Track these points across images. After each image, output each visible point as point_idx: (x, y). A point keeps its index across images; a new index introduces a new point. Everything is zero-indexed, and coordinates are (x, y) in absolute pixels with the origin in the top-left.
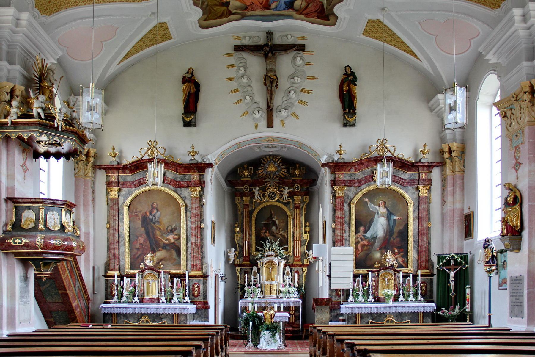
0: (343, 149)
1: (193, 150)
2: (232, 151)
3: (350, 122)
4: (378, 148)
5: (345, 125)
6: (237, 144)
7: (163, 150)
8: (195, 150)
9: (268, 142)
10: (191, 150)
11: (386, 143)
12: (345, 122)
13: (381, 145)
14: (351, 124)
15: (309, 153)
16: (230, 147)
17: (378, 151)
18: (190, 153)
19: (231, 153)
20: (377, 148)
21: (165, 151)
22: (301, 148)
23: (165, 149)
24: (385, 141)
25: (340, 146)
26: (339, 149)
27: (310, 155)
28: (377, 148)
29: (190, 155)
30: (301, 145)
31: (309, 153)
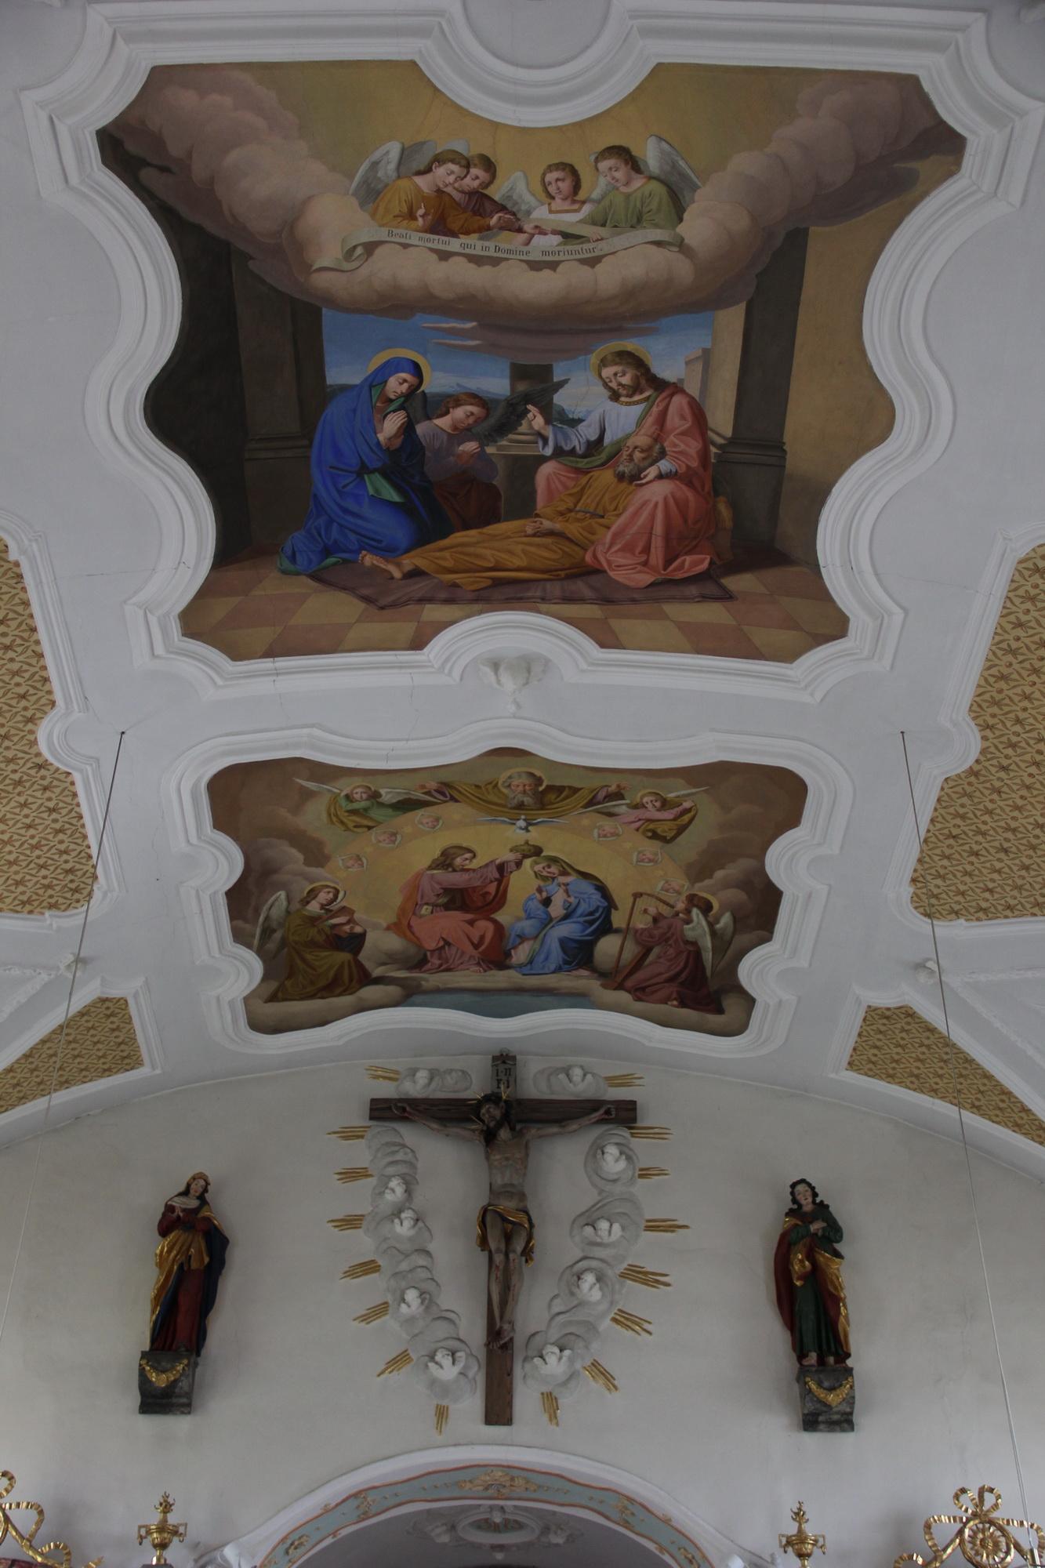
0: (810, 1530)
1: (165, 1520)
2: (334, 1534)
3: (829, 1407)
4: (967, 1532)
5: (810, 1423)
6: (355, 1495)
7: (33, 1514)
8: (173, 1519)
9: (491, 1492)
10: (154, 1519)
11: (996, 1506)
12: (810, 1407)
13: (975, 1515)
14: (836, 1417)
15: (662, 1549)
16: (327, 1510)
17: (968, 1546)
18: (149, 1533)
19: (329, 1541)
20: (961, 1532)
21: (39, 1523)
22: (626, 1524)
23: (41, 1513)
24: (989, 1499)
25: (799, 1515)
26: (792, 1529)
27: (666, 1558)
28: (961, 1532)
29: (147, 1542)
30: (629, 1507)
31: (662, 1549)
